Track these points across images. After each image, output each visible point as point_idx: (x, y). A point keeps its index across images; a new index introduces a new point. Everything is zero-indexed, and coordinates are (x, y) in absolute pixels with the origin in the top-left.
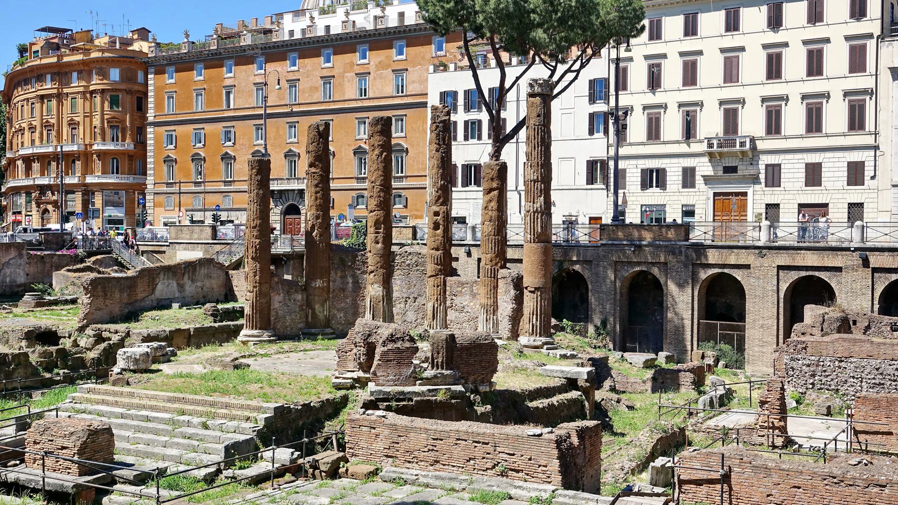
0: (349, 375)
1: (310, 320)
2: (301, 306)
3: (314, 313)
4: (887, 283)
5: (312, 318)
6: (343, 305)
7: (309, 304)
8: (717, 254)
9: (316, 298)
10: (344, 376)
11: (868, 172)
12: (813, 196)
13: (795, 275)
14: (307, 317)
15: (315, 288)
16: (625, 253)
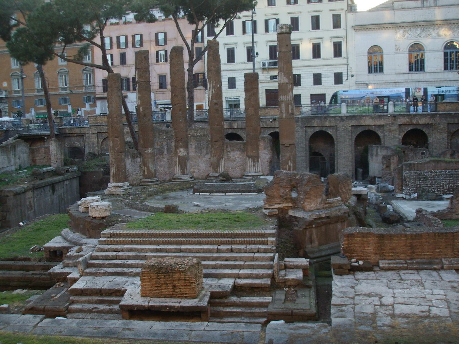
0: (277, 206)
1: (146, 173)
2: (140, 166)
5: (147, 172)
6: (162, 163)
7: (145, 164)
8: (319, 121)
9: (150, 160)
10: (273, 207)
11: (344, 78)
12: (318, 90)
13: (360, 130)
14: (144, 171)
15: (148, 154)
16: (266, 123)
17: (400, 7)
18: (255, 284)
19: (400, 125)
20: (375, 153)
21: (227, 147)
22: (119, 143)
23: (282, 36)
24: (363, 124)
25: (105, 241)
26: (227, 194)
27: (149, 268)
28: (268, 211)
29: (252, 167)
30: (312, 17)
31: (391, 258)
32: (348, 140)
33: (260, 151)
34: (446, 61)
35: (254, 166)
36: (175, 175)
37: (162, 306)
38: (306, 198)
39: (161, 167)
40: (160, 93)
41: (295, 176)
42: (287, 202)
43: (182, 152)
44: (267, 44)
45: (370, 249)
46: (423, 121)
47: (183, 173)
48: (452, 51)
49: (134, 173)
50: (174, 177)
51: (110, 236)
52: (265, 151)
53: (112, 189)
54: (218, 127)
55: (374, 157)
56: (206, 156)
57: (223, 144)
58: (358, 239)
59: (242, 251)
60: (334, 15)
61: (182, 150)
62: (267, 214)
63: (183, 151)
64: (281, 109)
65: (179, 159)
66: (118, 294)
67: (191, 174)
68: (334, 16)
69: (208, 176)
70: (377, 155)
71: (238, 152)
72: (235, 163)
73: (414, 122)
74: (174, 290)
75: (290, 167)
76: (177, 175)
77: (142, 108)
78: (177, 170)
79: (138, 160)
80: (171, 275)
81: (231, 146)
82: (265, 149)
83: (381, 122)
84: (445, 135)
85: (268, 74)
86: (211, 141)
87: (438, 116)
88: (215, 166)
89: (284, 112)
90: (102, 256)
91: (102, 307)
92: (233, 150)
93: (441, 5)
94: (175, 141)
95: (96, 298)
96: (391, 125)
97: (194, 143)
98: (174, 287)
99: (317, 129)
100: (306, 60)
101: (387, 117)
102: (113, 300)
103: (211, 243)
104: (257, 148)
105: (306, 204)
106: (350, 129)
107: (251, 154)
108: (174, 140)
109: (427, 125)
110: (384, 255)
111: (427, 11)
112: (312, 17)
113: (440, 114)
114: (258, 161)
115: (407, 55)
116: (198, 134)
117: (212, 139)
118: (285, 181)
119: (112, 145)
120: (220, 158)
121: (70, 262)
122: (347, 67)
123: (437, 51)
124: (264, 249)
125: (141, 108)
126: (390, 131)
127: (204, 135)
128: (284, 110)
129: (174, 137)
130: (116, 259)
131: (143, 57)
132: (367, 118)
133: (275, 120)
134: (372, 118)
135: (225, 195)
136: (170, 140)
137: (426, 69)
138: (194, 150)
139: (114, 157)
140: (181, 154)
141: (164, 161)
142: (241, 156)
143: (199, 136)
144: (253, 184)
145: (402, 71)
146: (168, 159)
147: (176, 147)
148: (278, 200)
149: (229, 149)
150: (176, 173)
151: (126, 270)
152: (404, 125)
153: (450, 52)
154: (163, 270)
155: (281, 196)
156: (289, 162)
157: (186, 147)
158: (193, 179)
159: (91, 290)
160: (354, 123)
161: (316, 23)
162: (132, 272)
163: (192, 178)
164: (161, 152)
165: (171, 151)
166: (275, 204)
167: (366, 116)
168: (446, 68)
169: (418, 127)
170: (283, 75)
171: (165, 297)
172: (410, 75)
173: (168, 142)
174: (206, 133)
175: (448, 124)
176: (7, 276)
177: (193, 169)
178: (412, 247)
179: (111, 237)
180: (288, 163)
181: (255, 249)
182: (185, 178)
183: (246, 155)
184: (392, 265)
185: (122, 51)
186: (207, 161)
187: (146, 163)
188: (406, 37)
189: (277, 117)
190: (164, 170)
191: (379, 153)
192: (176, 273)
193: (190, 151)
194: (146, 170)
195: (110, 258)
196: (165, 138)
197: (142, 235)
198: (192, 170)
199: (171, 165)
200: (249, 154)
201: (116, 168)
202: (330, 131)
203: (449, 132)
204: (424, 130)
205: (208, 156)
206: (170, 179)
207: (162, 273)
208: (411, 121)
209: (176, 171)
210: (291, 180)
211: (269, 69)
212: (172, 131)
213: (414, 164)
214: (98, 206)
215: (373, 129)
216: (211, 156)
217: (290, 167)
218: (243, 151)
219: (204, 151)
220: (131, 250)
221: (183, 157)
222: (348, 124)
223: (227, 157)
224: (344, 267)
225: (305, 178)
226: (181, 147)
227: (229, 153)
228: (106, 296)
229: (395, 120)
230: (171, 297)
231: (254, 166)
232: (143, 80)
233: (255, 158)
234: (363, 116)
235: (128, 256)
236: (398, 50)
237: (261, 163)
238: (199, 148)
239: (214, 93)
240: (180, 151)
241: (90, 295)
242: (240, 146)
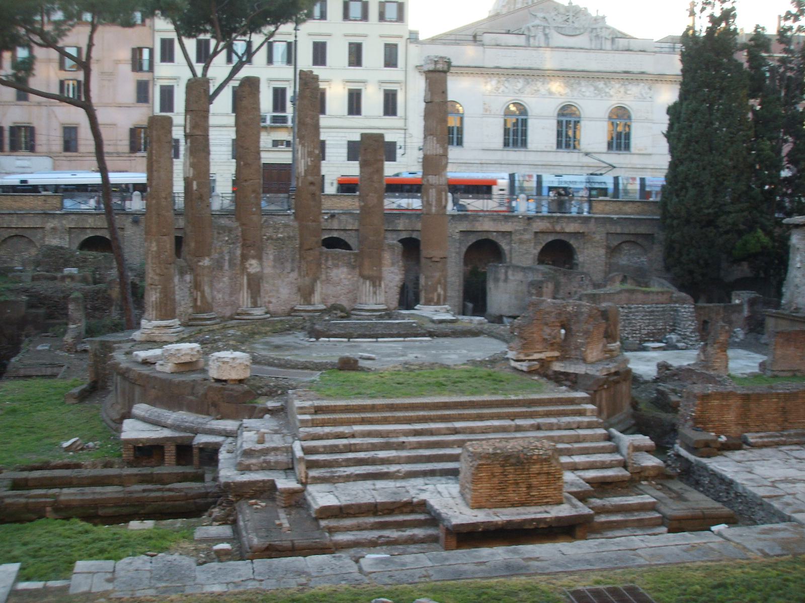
0: (536, 356)
1: (199, 303)
3: (203, 296)
4: (544, 244)
5: (202, 301)
6: (221, 284)
7: (197, 286)
8: (407, 221)
9: (206, 279)
11: (399, 152)
13: (472, 239)
14: (196, 300)
15: (203, 268)
17: (493, 42)
18: (609, 477)
19: (536, 233)
20: (502, 277)
21: (327, 260)
22: (168, 246)
23: (436, 75)
24: (480, 229)
25: (313, 420)
26: (380, 340)
27: (489, 458)
28: (524, 364)
29: (371, 294)
30: (350, 44)
31: (757, 429)
32: (454, 255)
33: (384, 269)
34: (559, 134)
35: (375, 293)
36: (240, 307)
37: (525, 521)
38: (588, 343)
39: (219, 292)
40: (64, 158)
41: (564, 307)
42: (552, 350)
43: (253, 266)
44: (380, 86)
45: (731, 416)
46: (571, 228)
47: (255, 305)
48: (568, 119)
49: (183, 303)
50: (239, 311)
51: (313, 410)
52: (392, 269)
53: (154, 331)
54: (314, 223)
55: (501, 284)
56: (291, 275)
57: (321, 254)
58: (716, 402)
59: (555, 428)
60: (386, 45)
61: (254, 262)
62: (525, 369)
63: (255, 265)
64: (428, 198)
65: (249, 280)
66: (408, 510)
67: (265, 306)
68: (387, 46)
69: (293, 310)
70: (506, 280)
71: (345, 270)
72: (339, 288)
73: (558, 228)
74: (528, 494)
75: (439, 295)
76: (244, 308)
77: (198, 185)
78: (244, 299)
79: (188, 278)
80: (526, 467)
81: (333, 259)
82: (393, 264)
83: (507, 227)
84: (602, 251)
85: (269, 137)
86: (301, 247)
87: (593, 220)
88: (306, 293)
89: (434, 203)
90: (325, 447)
91: (394, 534)
92: (337, 266)
93: (556, 46)
94: (243, 246)
95: (372, 520)
96: (522, 232)
97: (272, 251)
98: (529, 487)
100: (336, 117)
101: (516, 220)
102: (405, 521)
103: (499, 417)
104: (379, 264)
105: (588, 351)
106: (457, 236)
107: (371, 273)
108: (239, 245)
109: (576, 234)
110: (747, 425)
111: (534, 53)
112: (350, 44)
113: (596, 218)
114: (380, 286)
116: (280, 235)
117: (301, 244)
118: (553, 315)
119: (155, 249)
120: (315, 280)
121: (254, 461)
122: (405, 133)
123: (547, 117)
124: (588, 422)
126: (521, 242)
127: (289, 237)
128: (434, 200)
129: (241, 239)
130: (350, 451)
131: (202, 91)
132: (486, 219)
133: (333, 216)
134: (494, 220)
135: (377, 342)
136: (233, 243)
137: (633, 148)
138: (271, 263)
139: (158, 271)
140: (252, 270)
141: (224, 282)
142: (350, 277)
143: (279, 239)
144: (414, 323)
145: (492, 146)
146: (231, 278)
147: (244, 258)
148: (539, 347)
149: (330, 263)
150: (241, 303)
151: (384, 469)
152: (542, 232)
153: (567, 121)
154: (513, 461)
155: (545, 340)
156: (439, 286)
157: (260, 258)
158: (268, 315)
159: (359, 506)
160: (464, 226)
161: (356, 55)
162: (398, 471)
163: (267, 313)
164: (219, 265)
165: (235, 264)
166: (535, 352)
167: (485, 216)
168: (506, 144)
169: (562, 237)
170: (435, 142)
171: (513, 505)
172: (505, 153)
173: (230, 248)
174: (291, 234)
175: (608, 234)
176: (91, 497)
177: (269, 297)
178: (784, 411)
179: (316, 413)
180: (436, 290)
181: (574, 422)
182: (258, 312)
183: (358, 273)
184: (766, 440)
185: (144, 76)
186: (292, 283)
187: (200, 285)
188: (500, 91)
189: (336, 211)
190: (223, 299)
191: (511, 277)
192: (534, 464)
193: (265, 264)
194: (199, 298)
195: (340, 449)
196: (227, 241)
197: (373, 408)
198: (267, 299)
199: (234, 290)
200: (366, 272)
201: (160, 293)
203: (608, 247)
204: (571, 242)
205: (294, 275)
206: (232, 315)
207: (512, 465)
208: (553, 227)
209: (241, 299)
210: (560, 314)
211: (272, 127)
212: (237, 228)
213: (599, 295)
214: (234, 359)
215: (493, 237)
216: (300, 275)
217: (439, 295)
218: (354, 267)
219: (288, 266)
220: (369, 434)
221: (255, 274)
222: (456, 228)
223: (327, 276)
224: (713, 445)
225: (583, 310)
226: (253, 257)
227: (329, 271)
228: (384, 515)
229: (529, 224)
230: (522, 504)
231: (375, 293)
232: (200, 133)
233: (376, 281)
234: (480, 216)
235: (372, 444)
236: (487, 112)
237: (385, 288)
238: (280, 261)
239: (309, 164)
240: (251, 265)
241: (354, 515)
242: (350, 258)
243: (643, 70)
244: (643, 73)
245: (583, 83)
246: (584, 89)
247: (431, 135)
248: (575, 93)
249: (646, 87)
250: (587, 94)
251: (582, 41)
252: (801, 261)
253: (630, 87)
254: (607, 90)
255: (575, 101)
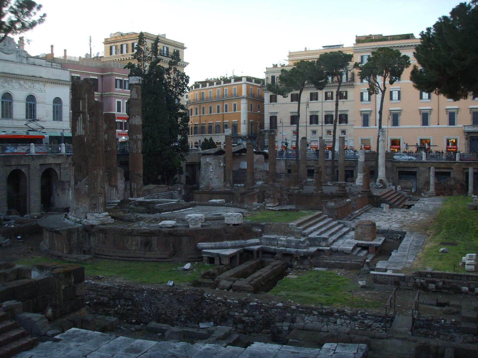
13: (44, 168)
24: (48, 162)
52: (121, 181)
83: (59, 161)
99: (14, 168)
106: (38, 167)
115: (25, 104)
119: (102, 174)
125: (85, 138)
126: (65, 169)
160: (41, 162)
202: (24, 170)
215: (53, 167)
243: (41, 76)
244: (41, 77)
245: (14, 81)
246: (14, 84)
247: (138, 115)
248: (10, 87)
249: (43, 85)
250: (16, 87)
251: (12, 57)
252: (213, 169)
253: (35, 84)
254: (25, 86)
255: (10, 91)
